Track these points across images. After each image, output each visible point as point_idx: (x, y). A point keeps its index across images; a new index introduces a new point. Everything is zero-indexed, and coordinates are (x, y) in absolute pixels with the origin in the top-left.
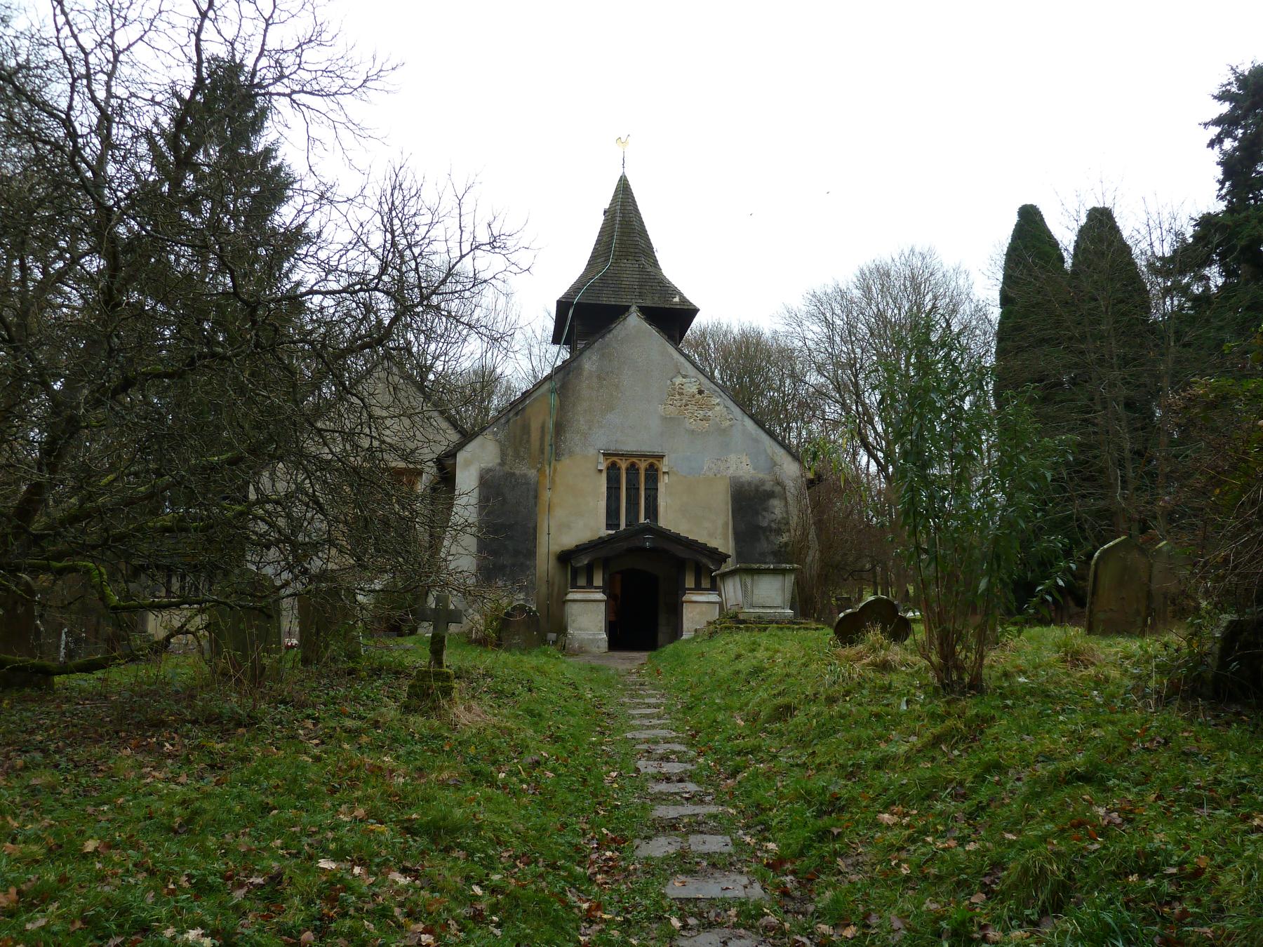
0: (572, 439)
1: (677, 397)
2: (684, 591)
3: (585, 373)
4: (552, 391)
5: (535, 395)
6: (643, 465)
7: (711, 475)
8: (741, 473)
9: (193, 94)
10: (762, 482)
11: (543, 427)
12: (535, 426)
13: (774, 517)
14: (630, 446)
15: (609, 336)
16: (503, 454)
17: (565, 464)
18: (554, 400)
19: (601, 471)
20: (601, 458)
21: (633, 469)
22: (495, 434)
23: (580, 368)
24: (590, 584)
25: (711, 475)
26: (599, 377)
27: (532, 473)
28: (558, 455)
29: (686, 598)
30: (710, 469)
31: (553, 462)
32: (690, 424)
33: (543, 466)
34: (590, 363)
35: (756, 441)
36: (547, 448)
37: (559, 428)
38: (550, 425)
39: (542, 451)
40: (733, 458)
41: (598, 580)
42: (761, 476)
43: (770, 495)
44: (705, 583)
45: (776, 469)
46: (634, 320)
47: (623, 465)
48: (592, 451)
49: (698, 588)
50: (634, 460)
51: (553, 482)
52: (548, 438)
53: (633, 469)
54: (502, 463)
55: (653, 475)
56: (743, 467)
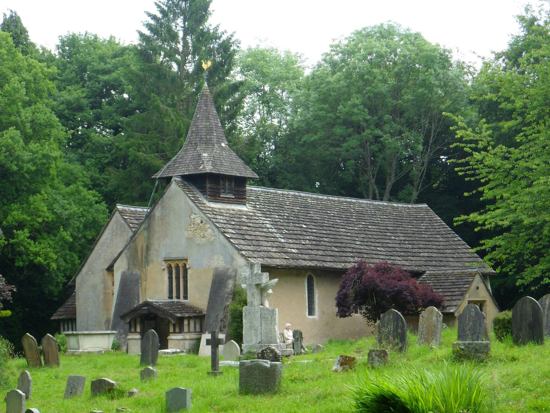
0: (152, 252)
1: (193, 226)
2: (168, 334)
3: (156, 218)
4: (145, 229)
5: (139, 232)
6: (181, 265)
7: (206, 267)
8: (219, 265)
9: (184, 24)
10: (228, 269)
11: (142, 248)
13: (227, 290)
14: (174, 255)
16: (129, 264)
17: (150, 268)
18: (145, 233)
19: (164, 269)
20: (164, 263)
21: (177, 267)
22: (126, 253)
23: (154, 215)
24: (135, 332)
25: (206, 267)
26: (162, 219)
27: (139, 272)
28: (147, 262)
29: (168, 338)
30: (206, 264)
31: (146, 267)
32: (199, 240)
34: (158, 212)
35: (225, 246)
36: (144, 259)
37: (148, 248)
38: (145, 247)
39: (142, 260)
40: (216, 257)
41: (138, 330)
42: (227, 266)
43: (229, 278)
44: (177, 330)
45: (234, 263)
46: (174, 187)
47: (173, 265)
48: (161, 259)
49: (174, 332)
50: (177, 262)
51: (146, 276)
53: (177, 267)
54: (129, 269)
55: (186, 271)
56: (219, 262)
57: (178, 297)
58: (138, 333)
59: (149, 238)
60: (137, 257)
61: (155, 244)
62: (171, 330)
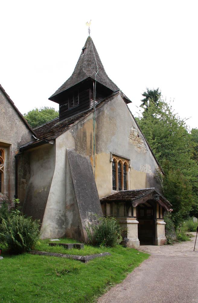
2: (156, 219)
12: (88, 134)
14: (120, 154)
15: (113, 101)
27: (88, 157)
28: (97, 151)
31: (95, 154)
33: (91, 155)
35: (152, 160)
36: (93, 146)
37: (97, 137)
39: (91, 147)
41: (135, 215)
44: (161, 217)
49: (160, 218)
50: (120, 159)
51: (95, 163)
52: (93, 141)
54: (76, 150)
57: (120, 189)
58: (135, 217)
59: (98, 128)
60: (86, 141)
61: (104, 136)
62: (158, 217)
